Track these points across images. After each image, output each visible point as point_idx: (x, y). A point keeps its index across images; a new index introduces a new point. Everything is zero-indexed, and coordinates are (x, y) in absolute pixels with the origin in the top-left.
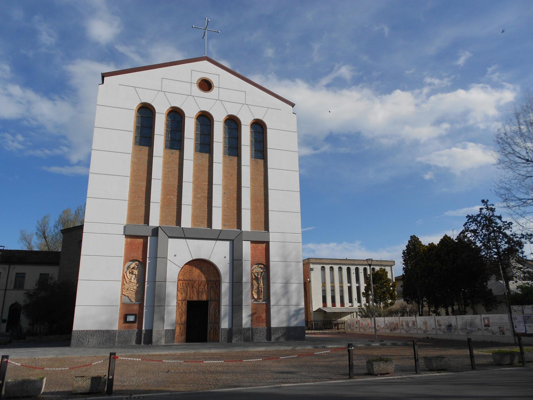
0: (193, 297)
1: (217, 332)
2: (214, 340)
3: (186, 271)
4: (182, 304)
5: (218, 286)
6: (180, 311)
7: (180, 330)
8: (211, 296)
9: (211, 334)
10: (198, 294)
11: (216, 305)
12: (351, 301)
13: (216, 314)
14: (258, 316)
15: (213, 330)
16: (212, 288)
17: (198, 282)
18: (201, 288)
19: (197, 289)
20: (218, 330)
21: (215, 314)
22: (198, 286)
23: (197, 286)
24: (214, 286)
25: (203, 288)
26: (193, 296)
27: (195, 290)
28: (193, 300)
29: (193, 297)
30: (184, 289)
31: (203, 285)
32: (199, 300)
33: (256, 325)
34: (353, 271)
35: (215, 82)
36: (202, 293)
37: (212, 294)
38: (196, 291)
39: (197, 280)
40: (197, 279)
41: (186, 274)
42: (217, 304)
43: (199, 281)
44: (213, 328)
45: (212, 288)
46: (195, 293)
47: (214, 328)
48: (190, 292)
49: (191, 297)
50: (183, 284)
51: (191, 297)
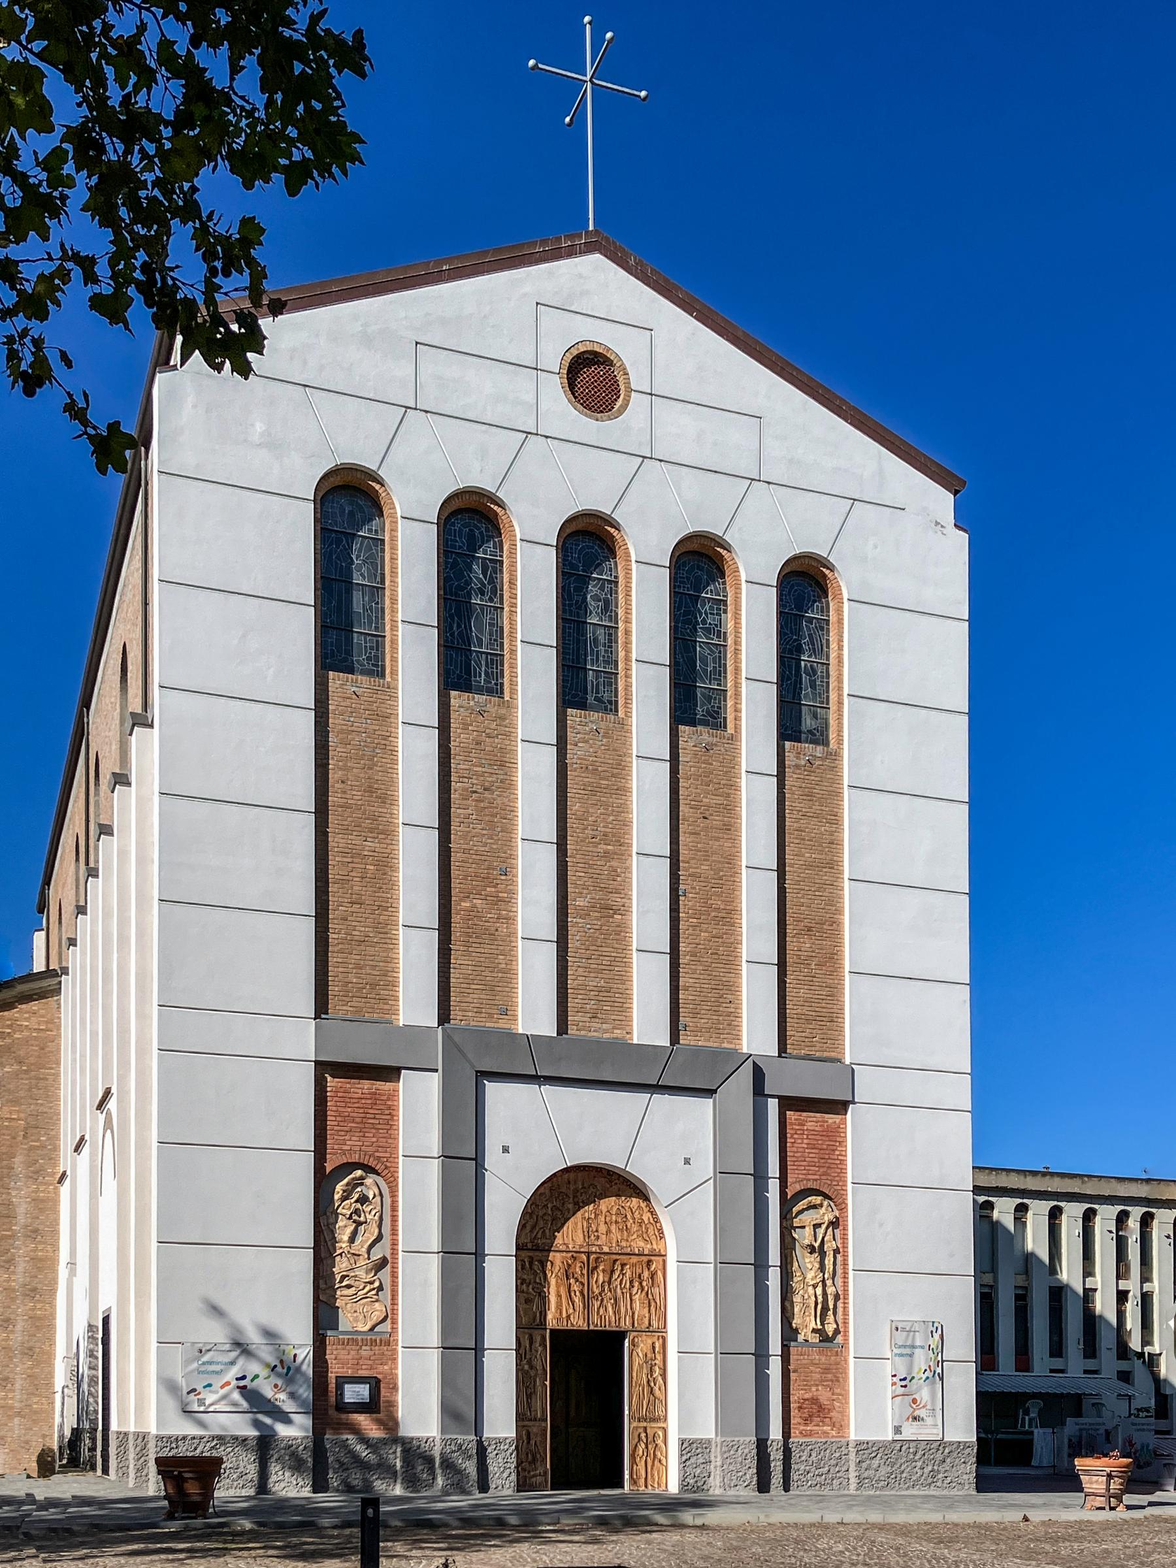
0: (568, 1317)
1: (659, 1454)
2: (649, 1482)
3: (541, 1214)
4: (531, 1344)
5: (660, 1274)
6: (526, 1367)
7: (528, 1443)
8: (633, 1313)
9: (638, 1459)
10: (587, 1307)
11: (654, 1348)
12: (1057, 1350)
13: (652, 1384)
14: (806, 1396)
15: (643, 1446)
16: (636, 1284)
17: (584, 1257)
18: (596, 1282)
19: (583, 1284)
20: (664, 1446)
21: (648, 1381)
22: (585, 1272)
23: (583, 1274)
24: (646, 1274)
25: (604, 1282)
26: (571, 1311)
27: (576, 1287)
28: (570, 1327)
29: (568, 1317)
30: (535, 1282)
31: (603, 1271)
32: (592, 1327)
33: (801, 1433)
34: (1133, 1224)
35: (554, 392)
36: (602, 1300)
37: (637, 1305)
38: (582, 1292)
39: (582, 1250)
40: (581, 1246)
41: (541, 1223)
42: (657, 1345)
43: (588, 1254)
44: (643, 1435)
45: (636, 1284)
46: (577, 1300)
47: (647, 1436)
48: (559, 1296)
49: (564, 1315)
50: (531, 1263)
51: (564, 1315)
